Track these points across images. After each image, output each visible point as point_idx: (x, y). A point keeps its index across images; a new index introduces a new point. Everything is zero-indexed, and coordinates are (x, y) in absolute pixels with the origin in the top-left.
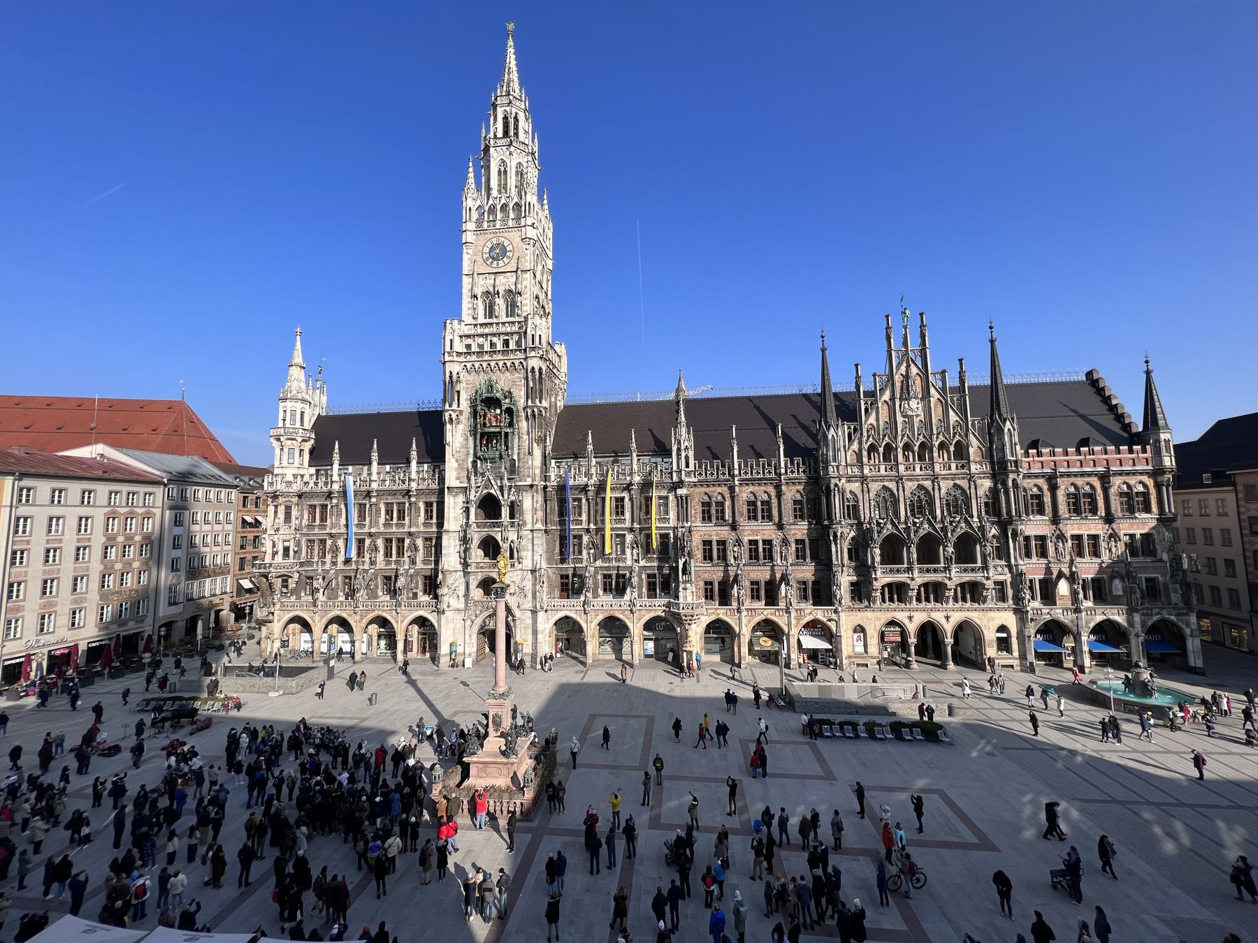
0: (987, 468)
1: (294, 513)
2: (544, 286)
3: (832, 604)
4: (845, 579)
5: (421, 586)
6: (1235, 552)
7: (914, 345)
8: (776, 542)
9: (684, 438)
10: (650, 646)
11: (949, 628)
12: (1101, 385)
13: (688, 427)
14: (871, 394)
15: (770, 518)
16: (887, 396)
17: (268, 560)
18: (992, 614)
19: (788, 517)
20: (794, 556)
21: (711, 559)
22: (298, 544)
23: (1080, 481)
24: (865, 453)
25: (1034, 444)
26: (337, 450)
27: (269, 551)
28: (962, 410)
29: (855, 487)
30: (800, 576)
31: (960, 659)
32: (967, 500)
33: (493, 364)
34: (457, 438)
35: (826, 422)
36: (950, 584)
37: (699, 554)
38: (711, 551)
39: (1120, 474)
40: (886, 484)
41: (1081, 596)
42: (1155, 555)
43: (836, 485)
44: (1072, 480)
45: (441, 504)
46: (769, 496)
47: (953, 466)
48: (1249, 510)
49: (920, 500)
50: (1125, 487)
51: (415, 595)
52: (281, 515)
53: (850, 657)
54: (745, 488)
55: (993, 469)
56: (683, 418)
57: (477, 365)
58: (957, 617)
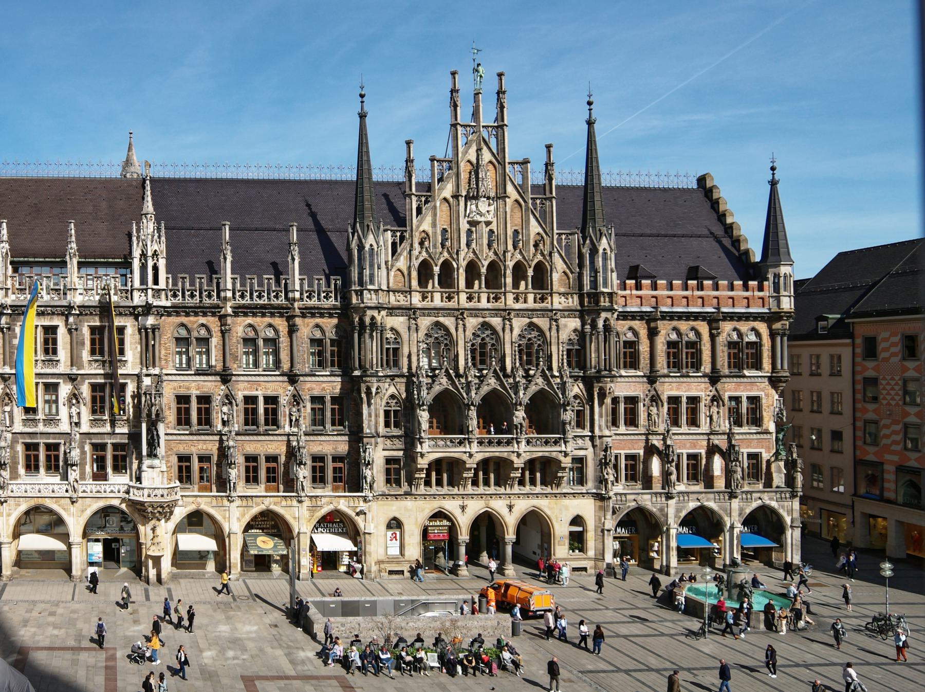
0: (573, 302)
3: (359, 489)
4: (377, 454)
6: (844, 423)
7: (487, 117)
8: (284, 400)
10: (97, 550)
11: (511, 521)
12: (715, 196)
13: (158, 221)
14: (428, 187)
15: (277, 363)
16: (448, 190)
18: (566, 502)
19: (305, 361)
20: (308, 421)
21: (188, 422)
23: (684, 326)
24: (414, 274)
25: (633, 274)
28: (543, 219)
29: (398, 322)
31: (518, 559)
32: (546, 343)
35: (362, 223)
36: (518, 463)
37: (171, 416)
38: (188, 411)
39: (732, 319)
40: (441, 319)
41: (674, 477)
44: (675, 323)
47: (531, 297)
49: (483, 345)
50: (735, 337)
53: (379, 562)
54: (240, 319)
55: (581, 303)
58: (522, 506)
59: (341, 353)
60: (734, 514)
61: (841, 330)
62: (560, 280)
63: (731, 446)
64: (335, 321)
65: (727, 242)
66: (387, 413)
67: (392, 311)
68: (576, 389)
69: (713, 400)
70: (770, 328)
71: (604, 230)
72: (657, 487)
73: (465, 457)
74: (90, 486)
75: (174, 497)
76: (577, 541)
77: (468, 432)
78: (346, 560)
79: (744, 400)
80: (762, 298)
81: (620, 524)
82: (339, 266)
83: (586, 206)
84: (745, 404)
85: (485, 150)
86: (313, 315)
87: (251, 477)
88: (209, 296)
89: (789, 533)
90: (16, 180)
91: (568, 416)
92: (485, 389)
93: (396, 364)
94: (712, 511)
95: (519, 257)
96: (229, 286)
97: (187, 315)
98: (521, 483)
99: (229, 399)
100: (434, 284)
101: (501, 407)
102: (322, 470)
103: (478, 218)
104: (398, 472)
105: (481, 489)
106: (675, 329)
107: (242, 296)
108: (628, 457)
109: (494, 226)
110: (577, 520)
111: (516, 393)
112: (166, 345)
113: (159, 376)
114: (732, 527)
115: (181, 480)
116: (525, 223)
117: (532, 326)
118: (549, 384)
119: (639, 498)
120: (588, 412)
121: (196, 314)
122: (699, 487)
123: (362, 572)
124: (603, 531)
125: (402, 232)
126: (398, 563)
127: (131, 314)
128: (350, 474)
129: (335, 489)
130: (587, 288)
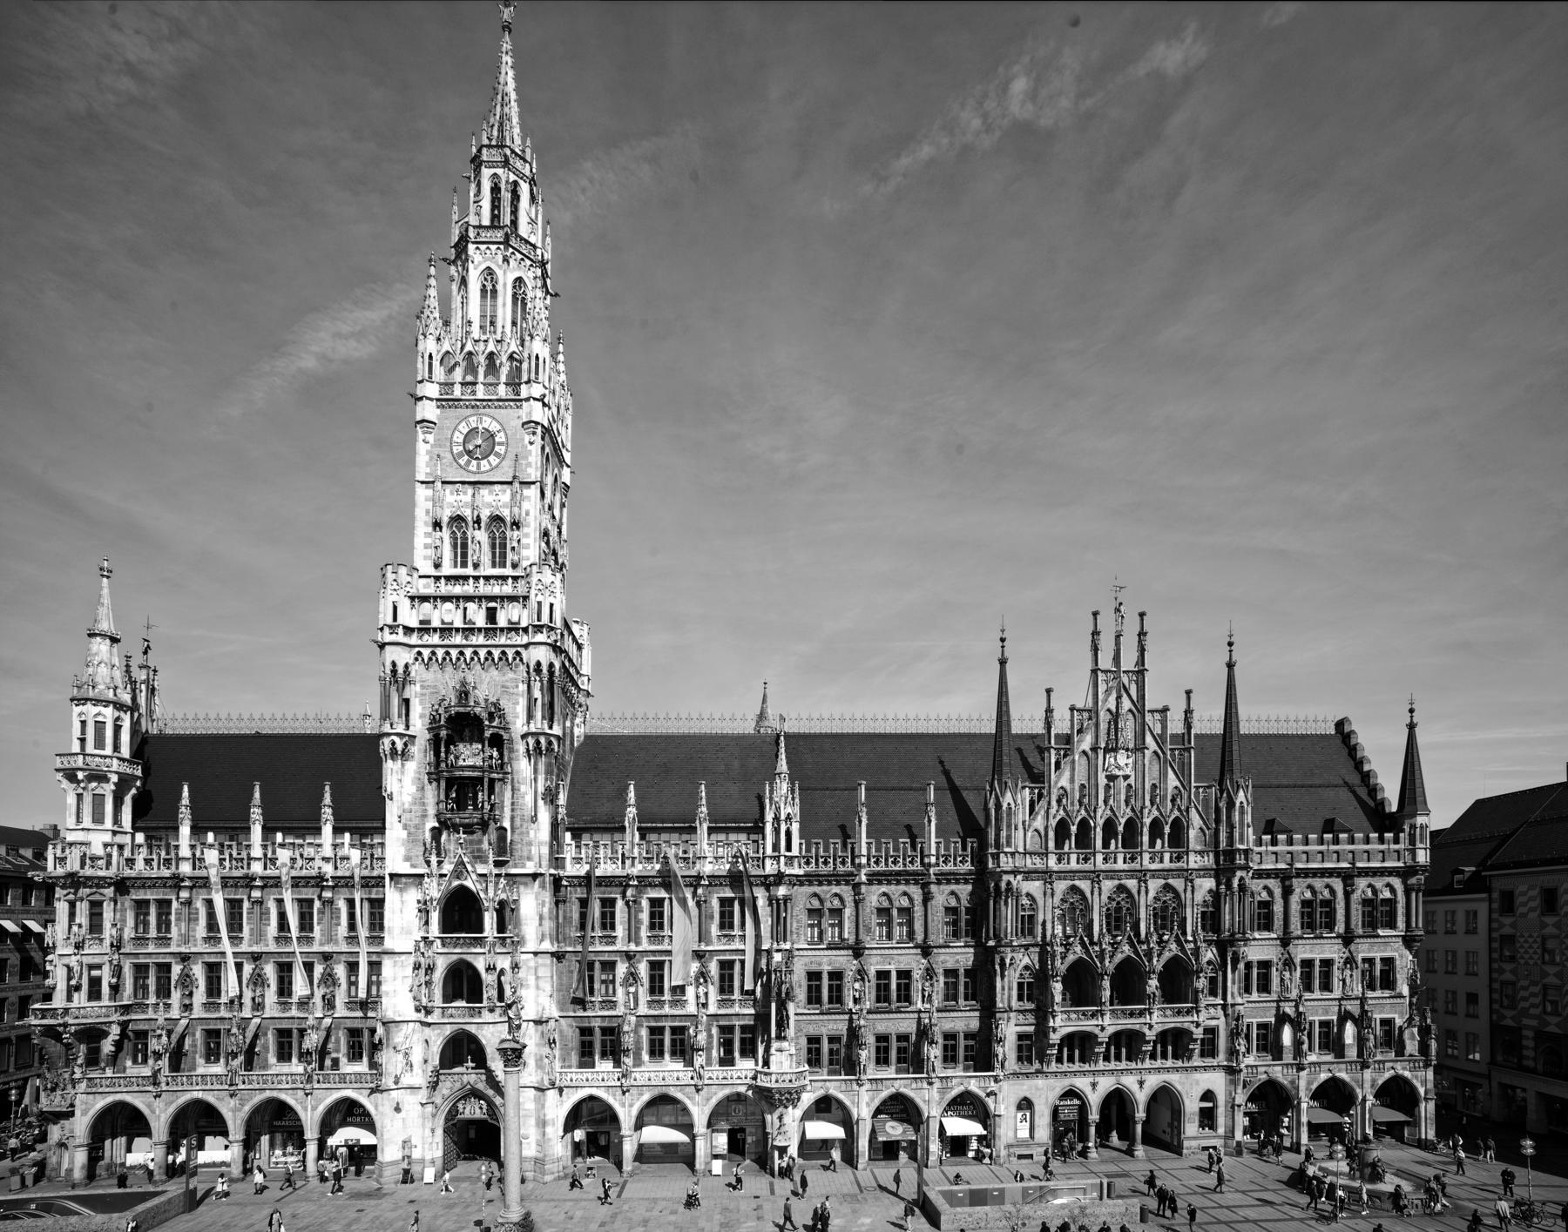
0: (1209, 861)
1: (108, 914)
2: (557, 512)
3: (991, 1068)
4: (1010, 1030)
5: (344, 1048)
6: (1480, 985)
7: (1129, 662)
9: (783, 799)
11: (1141, 1097)
14: (1068, 739)
15: (911, 935)
16: (1086, 743)
17: (59, 1001)
18: (1197, 1076)
20: (941, 996)
21: (819, 1001)
22: (118, 971)
23: (1318, 883)
24: (1051, 834)
25: (1269, 827)
26: (185, 800)
27: (61, 986)
28: (1182, 773)
29: (1034, 887)
30: (948, 1026)
31: (1150, 1140)
32: (1181, 905)
33: (468, 652)
34: (405, 785)
36: (1150, 1035)
37: (801, 994)
40: (1077, 883)
41: (1305, 1047)
42: (1393, 989)
43: (1009, 883)
44: (1309, 881)
45: (377, 905)
46: (911, 900)
47: (1167, 856)
48: (1502, 926)
51: (336, 1062)
52: (82, 917)
53: (1009, 1146)
54: (874, 888)
55: (1217, 862)
56: (783, 766)
57: (440, 653)
58: (1153, 1081)
59: (975, 921)
60: (1366, 1084)
61: (1476, 884)
62: (1196, 837)
63: (1364, 1012)
64: (969, 887)
65: (1362, 792)
66: (1020, 985)
67: (1029, 875)
68: (1209, 954)
69: (1345, 963)
70: (1404, 883)
71: (1241, 782)
72: (1288, 1057)
73: (1097, 1031)
74: (716, 1072)
75: (803, 1082)
76: (1207, 1118)
77: (1102, 1004)
78: (974, 1145)
79: (1378, 961)
80: (1398, 851)
81: (1251, 1099)
82: (975, 829)
83: (1226, 756)
84: (1378, 966)
85: (1125, 699)
86: (949, 882)
87: (882, 1059)
88: (843, 863)
89: (1423, 1105)
90: (644, 737)
91: (1202, 983)
92: (1119, 957)
93: (1031, 932)
94: (1343, 1082)
95: (1156, 813)
96: (864, 851)
97: (821, 884)
98: (1153, 1057)
99: (861, 974)
100: (1070, 845)
101: (1131, 976)
102: (954, 1048)
103: (1116, 772)
104: (1029, 1049)
105: (1113, 1065)
106: (1310, 887)
107: (877, 863)
108: (1260, 1026)
109: (1131, 781)
110: (1208, 1096)
111: (1150, 961)
112: (798, 918)
113: (790, 951)
114: (1364, 1100)
115: (810, 1062)
116: (1163, 776)
117: (1168, 888)
118: (1183, 949)
119: (1270, 1070)
120: (1220, 979)
121: (830, 883)
122: (1330, 1058)
123: (991, 1157)
124: (1233, 1107)
125: (1041, 789)
126: (1028, 1146)
127: (763, 884)
128: (981, 1053)
129: (966, 1069)
130: (1223, 845)
